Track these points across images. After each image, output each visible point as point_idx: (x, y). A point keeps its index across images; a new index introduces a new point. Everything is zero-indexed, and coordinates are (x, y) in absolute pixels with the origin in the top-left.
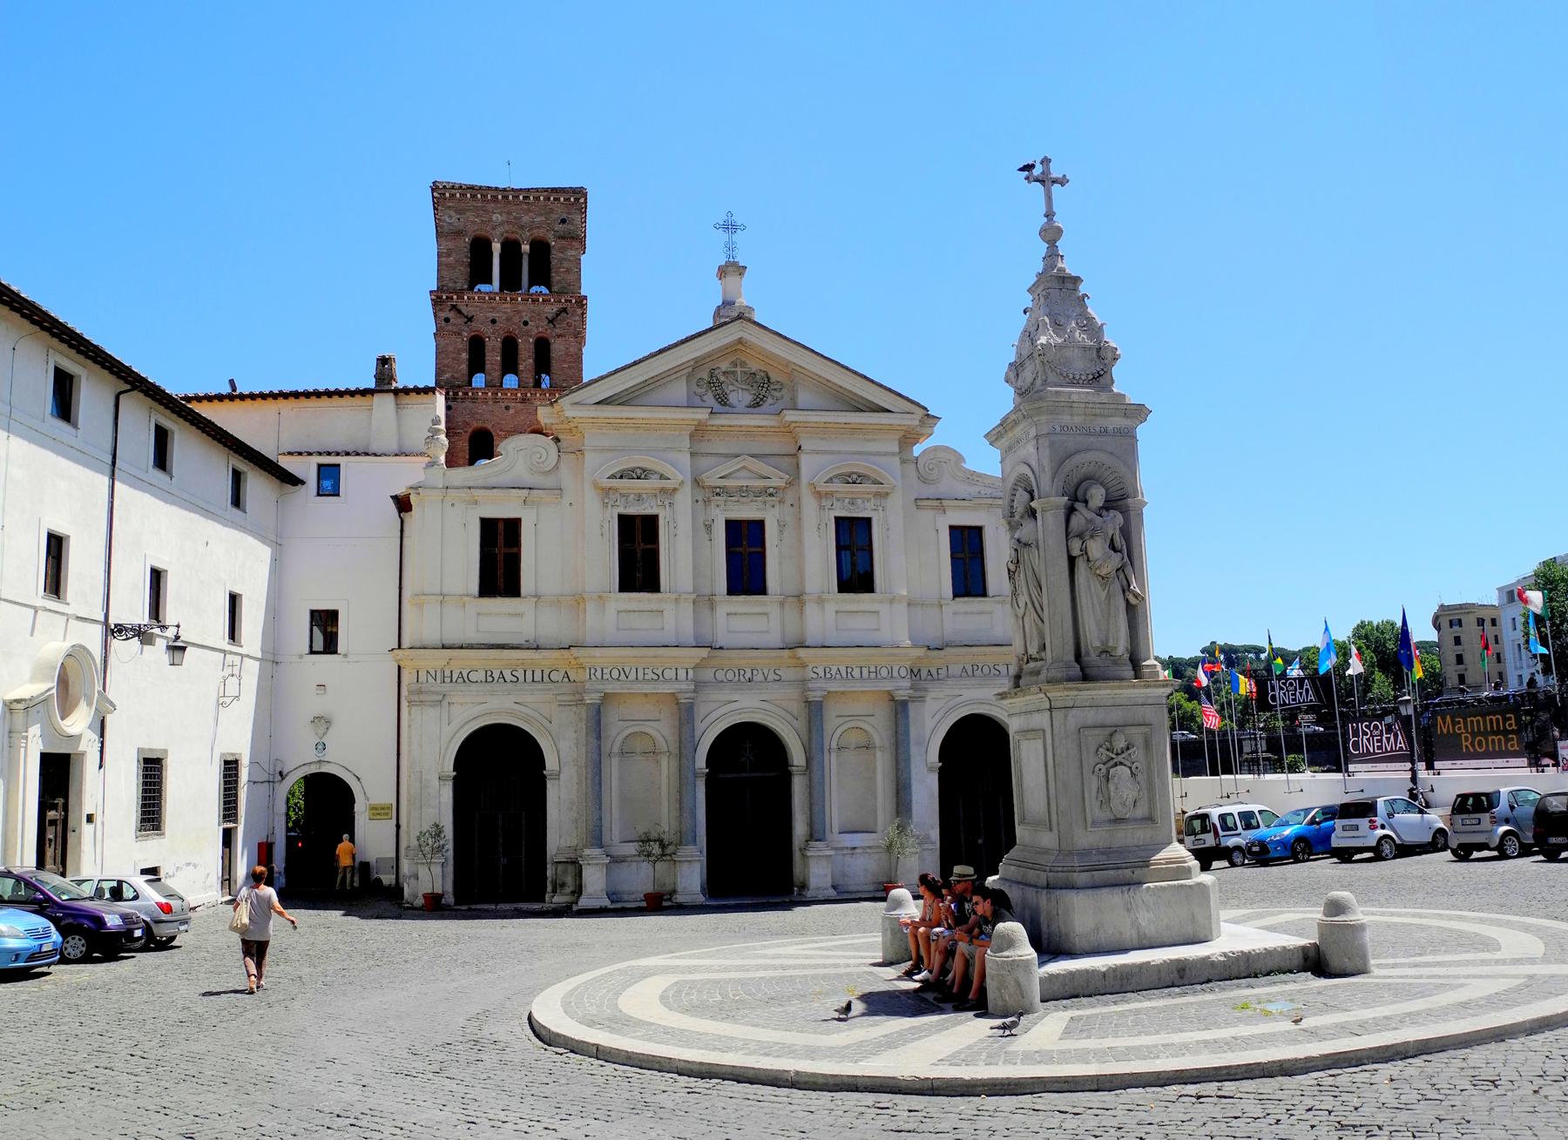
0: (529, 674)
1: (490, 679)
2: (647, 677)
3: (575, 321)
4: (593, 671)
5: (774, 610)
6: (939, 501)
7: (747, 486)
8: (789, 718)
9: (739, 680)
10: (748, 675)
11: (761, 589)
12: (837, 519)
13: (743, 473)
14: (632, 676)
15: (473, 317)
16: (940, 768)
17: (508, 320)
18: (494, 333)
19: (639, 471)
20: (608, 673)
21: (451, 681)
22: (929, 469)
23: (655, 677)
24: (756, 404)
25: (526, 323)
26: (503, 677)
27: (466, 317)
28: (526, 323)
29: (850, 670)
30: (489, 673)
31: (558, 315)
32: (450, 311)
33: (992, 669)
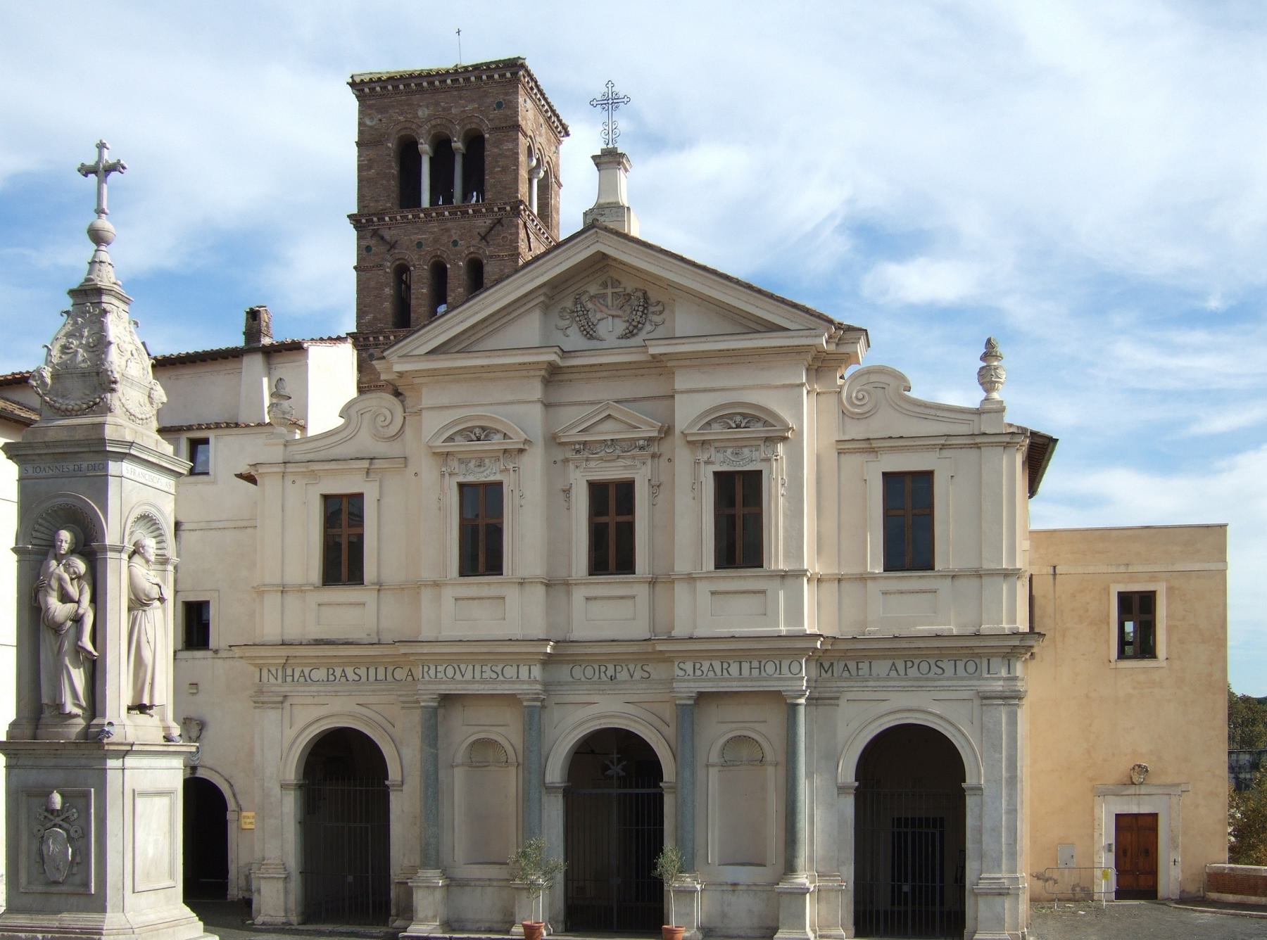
0: (372, 671)
1: (332, 678)
2: (485, 676)
3: (511, 234)
4: (426, 669)
5: (642, 592)
6: (868, 442)
7: (612, 440)
8: (658, 723)
9: (600, 678)
10: (610, 672)
11: (626, 565)
12: (717, 475)
13: (609, 426)
14: (468, 676)
15: (396, 242)
16: (857, 789)
17: (436, 241)
18: (419, 259)
19: (477, 431)
20: (443, 672)
21: (293, 681)
22: (857, 399)
23: (494, 676)
24: (629, 334)
25: (455, 243)
26: (345, 676)
27: (388, 243)
28: (455, 243)
29: (725, 665)
30: (331, 671)
31: (491, 229)
32: (371, 237)
33: (933, 667)
